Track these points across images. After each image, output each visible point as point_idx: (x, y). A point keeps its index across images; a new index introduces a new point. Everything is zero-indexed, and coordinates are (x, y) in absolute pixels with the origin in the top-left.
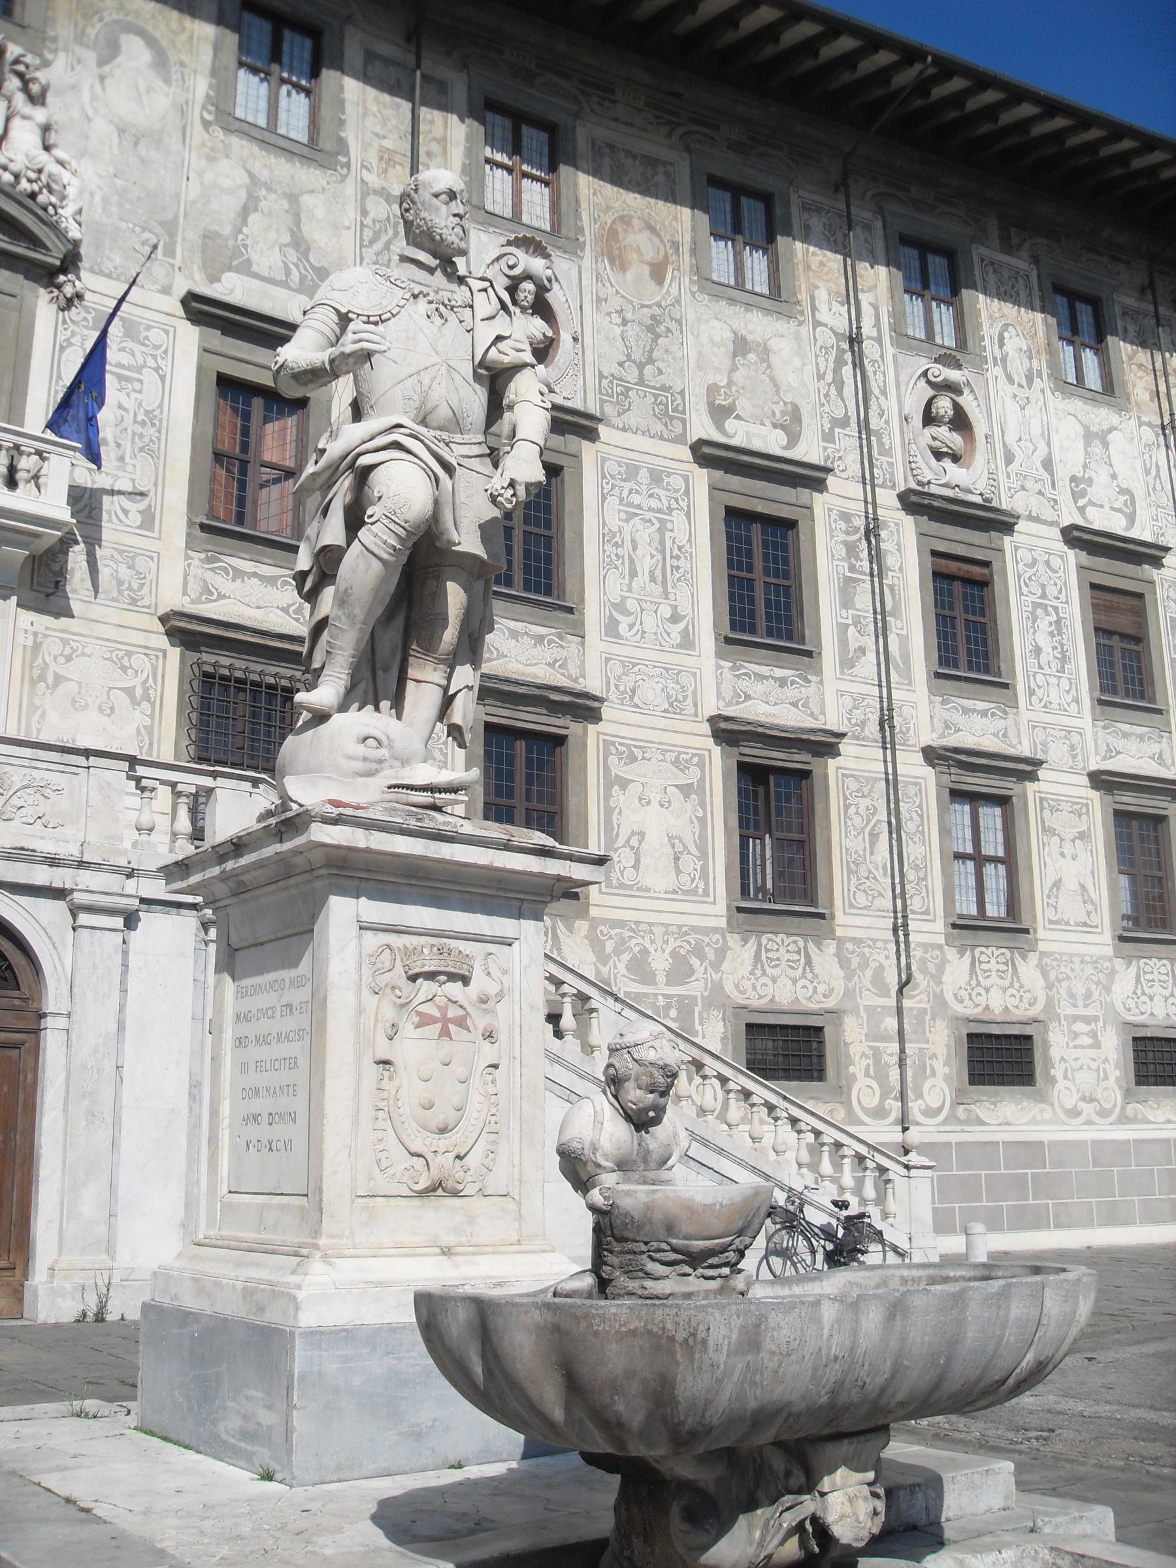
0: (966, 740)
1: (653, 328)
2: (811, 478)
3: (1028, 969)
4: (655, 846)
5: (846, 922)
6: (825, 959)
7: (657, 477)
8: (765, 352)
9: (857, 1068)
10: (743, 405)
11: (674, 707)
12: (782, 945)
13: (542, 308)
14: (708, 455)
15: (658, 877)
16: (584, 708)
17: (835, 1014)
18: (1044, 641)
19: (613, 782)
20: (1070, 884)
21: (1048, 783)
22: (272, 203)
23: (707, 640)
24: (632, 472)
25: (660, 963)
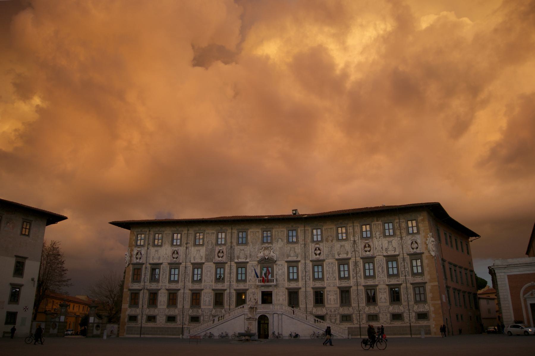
0: (369, 284)
1: (332, 248)
2: (349, 259)
3: (377, 308)
4: (332, 299)
5: (353, 305)
6: (351, 309)
7: (332, 263)
8: (344, 246)
9: (354, 319)
10: (342, 253)
11: (334, 286)
12: (346, 308)
13: (319, 249)
14: (337, 260)
15: (332, 303)
16: (324, 288)
17: (352, 314)
18: (380, 270)
19: (328, 294)
20: (383, 298)
21: (380, 287)
22: (293, 249)
23: (337, 279)
24: (329, 263)
25: (333, 311)
